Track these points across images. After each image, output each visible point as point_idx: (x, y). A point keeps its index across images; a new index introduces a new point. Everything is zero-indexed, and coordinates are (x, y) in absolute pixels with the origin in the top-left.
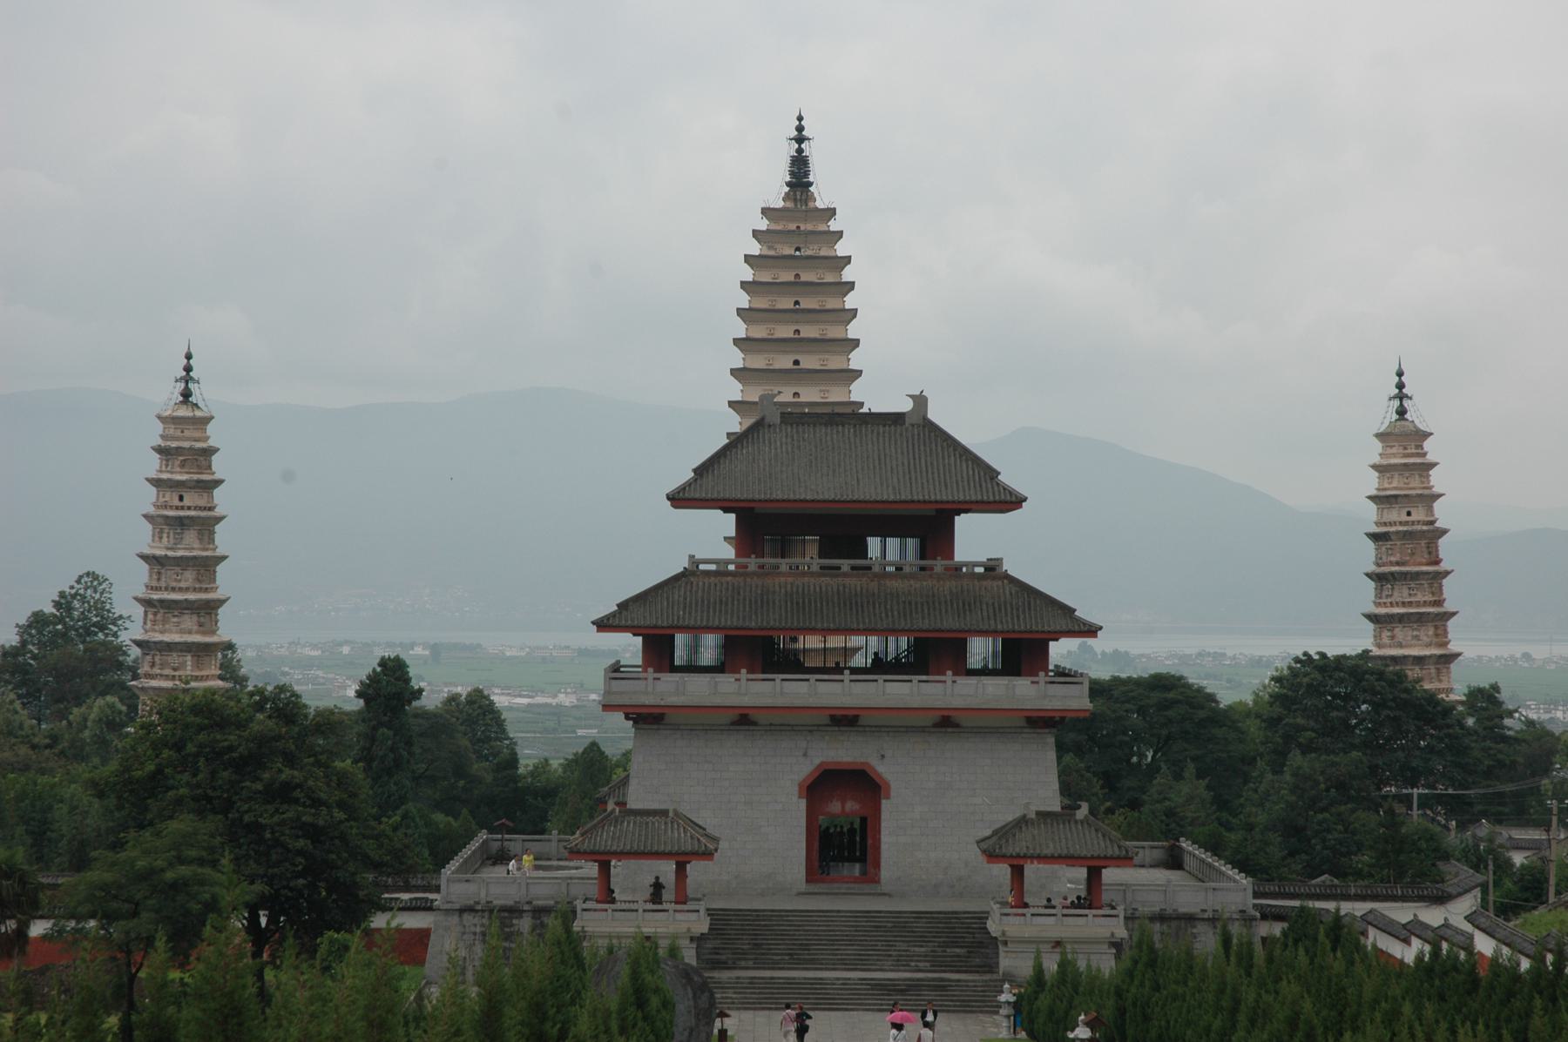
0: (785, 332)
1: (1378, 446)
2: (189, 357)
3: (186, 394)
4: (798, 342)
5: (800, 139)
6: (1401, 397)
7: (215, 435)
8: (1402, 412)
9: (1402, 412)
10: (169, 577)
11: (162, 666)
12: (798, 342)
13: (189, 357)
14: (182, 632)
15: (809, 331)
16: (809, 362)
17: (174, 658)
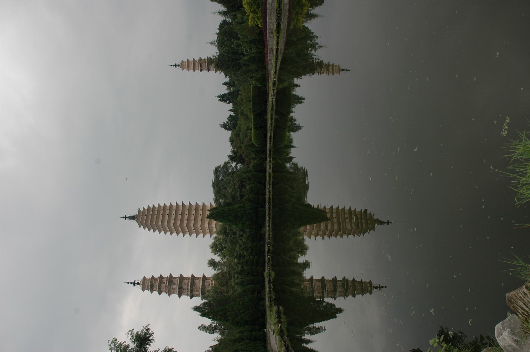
0: (161, 217)
1: (185, 70)
2: (128, 283)
3: (138, 284)
4: (163, 215)
5: (125, 218)
6: (176, 65)
7: (148, 276)
8: (178, 65)
9: (178, 65)
10: (185, 287)
11: (208, 287)
12: (163, 215)
13: (128, 283)
14: (200, 283)
15: (162, 212)
16: (167, 212)
17: (206, 284)
